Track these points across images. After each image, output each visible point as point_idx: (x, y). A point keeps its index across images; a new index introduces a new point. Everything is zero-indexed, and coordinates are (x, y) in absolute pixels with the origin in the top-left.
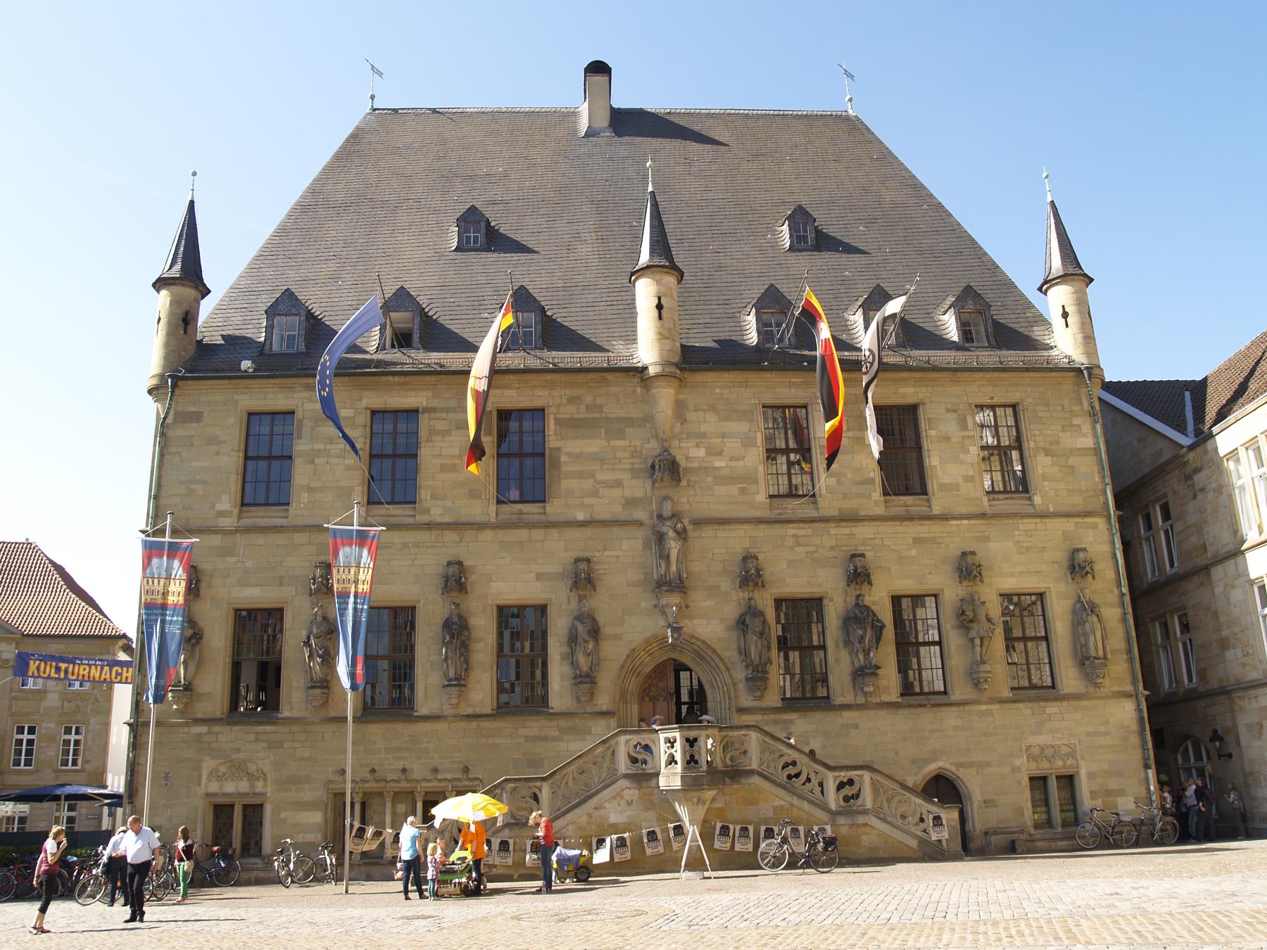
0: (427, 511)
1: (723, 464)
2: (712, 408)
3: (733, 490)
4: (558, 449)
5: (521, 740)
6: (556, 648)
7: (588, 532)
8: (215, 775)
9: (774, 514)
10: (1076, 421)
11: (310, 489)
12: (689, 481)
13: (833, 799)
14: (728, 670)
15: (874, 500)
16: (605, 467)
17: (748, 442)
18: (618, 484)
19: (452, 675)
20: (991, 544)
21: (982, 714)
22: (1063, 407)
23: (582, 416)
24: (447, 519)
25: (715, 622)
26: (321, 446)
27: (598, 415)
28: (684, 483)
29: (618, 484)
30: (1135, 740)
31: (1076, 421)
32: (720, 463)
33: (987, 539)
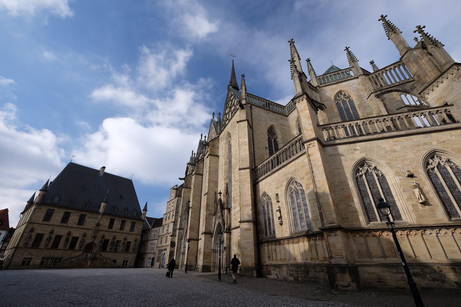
6: (78, 242)
8: (26, 255)
15: (118, 231)
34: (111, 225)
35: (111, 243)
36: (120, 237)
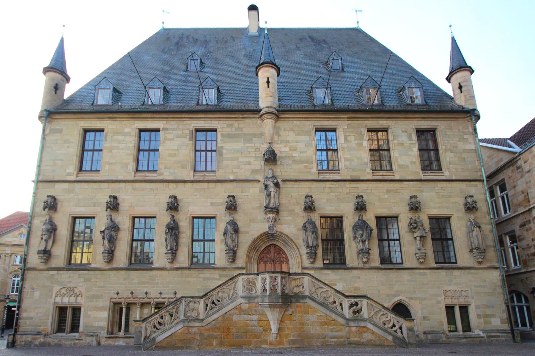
0: (162, 174)
1: (297, 155)
2: (292, 130)
3: (302, 166)
4: (222, 147)
5: (201, 280)
7: (235, 184)
9: (320, 178)
10: (465, 137)
11: (109, 164)
12: (281, 162)
13: (347, 312)
14: (298, 249)
16: (243, 155)
17: (308, 145)
18: (249, 163)
19: (169, 248)
20: (424, 194)
21: (421, 274)
22: (459, 130)
23: (233, 133)
24: (171, 178)
25: (292, 226)
26: (116, 145)
27: (240, 132)
28: (278, 163)
29: (249, 163)
30: (500, 290)
31: (465, 137)
32: (295, 154)
33: (422, 191)
35: (356, 228)
36: (385, 200)
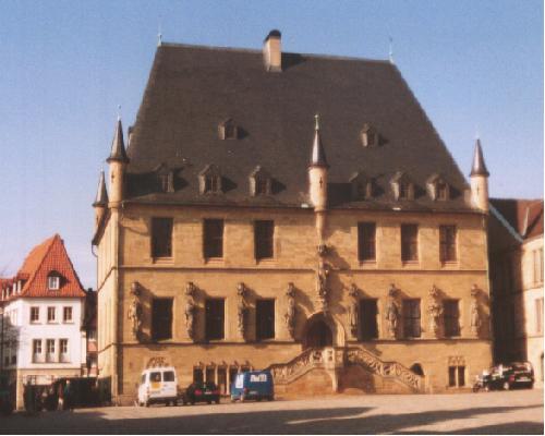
18: (303, 253)
34: (366, 251)
